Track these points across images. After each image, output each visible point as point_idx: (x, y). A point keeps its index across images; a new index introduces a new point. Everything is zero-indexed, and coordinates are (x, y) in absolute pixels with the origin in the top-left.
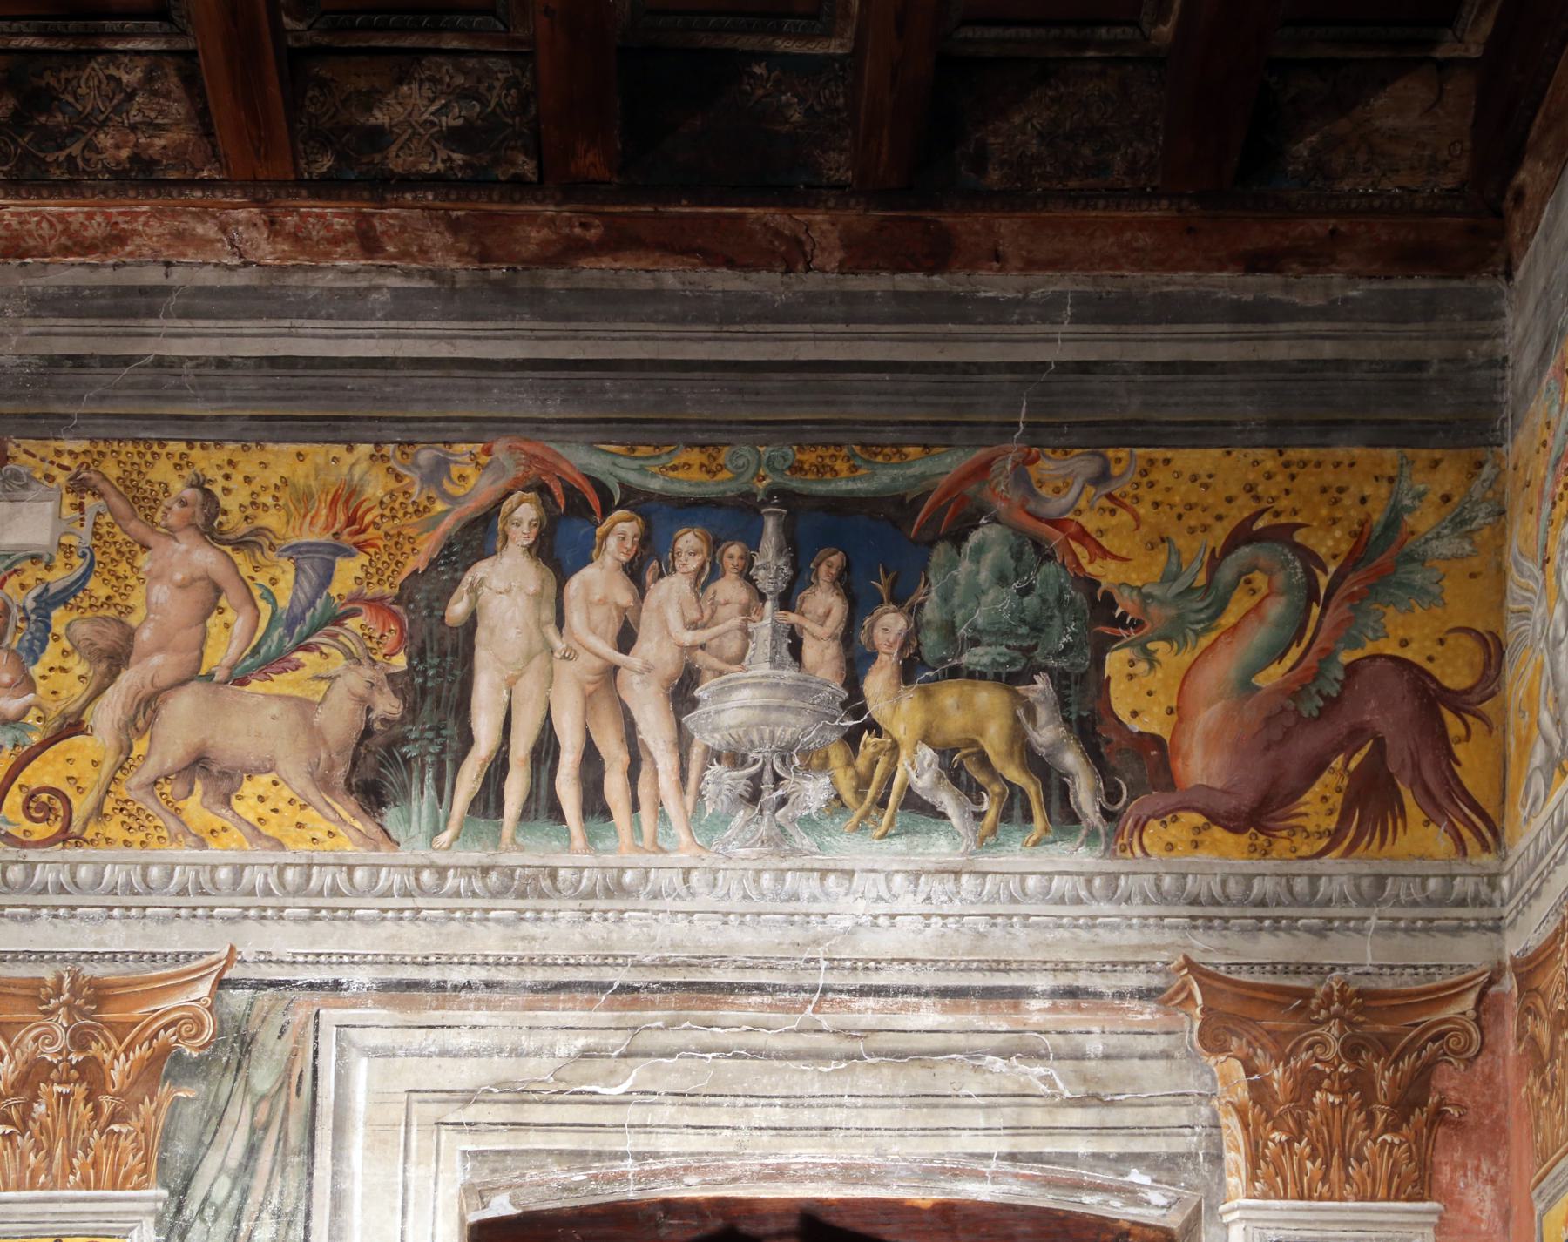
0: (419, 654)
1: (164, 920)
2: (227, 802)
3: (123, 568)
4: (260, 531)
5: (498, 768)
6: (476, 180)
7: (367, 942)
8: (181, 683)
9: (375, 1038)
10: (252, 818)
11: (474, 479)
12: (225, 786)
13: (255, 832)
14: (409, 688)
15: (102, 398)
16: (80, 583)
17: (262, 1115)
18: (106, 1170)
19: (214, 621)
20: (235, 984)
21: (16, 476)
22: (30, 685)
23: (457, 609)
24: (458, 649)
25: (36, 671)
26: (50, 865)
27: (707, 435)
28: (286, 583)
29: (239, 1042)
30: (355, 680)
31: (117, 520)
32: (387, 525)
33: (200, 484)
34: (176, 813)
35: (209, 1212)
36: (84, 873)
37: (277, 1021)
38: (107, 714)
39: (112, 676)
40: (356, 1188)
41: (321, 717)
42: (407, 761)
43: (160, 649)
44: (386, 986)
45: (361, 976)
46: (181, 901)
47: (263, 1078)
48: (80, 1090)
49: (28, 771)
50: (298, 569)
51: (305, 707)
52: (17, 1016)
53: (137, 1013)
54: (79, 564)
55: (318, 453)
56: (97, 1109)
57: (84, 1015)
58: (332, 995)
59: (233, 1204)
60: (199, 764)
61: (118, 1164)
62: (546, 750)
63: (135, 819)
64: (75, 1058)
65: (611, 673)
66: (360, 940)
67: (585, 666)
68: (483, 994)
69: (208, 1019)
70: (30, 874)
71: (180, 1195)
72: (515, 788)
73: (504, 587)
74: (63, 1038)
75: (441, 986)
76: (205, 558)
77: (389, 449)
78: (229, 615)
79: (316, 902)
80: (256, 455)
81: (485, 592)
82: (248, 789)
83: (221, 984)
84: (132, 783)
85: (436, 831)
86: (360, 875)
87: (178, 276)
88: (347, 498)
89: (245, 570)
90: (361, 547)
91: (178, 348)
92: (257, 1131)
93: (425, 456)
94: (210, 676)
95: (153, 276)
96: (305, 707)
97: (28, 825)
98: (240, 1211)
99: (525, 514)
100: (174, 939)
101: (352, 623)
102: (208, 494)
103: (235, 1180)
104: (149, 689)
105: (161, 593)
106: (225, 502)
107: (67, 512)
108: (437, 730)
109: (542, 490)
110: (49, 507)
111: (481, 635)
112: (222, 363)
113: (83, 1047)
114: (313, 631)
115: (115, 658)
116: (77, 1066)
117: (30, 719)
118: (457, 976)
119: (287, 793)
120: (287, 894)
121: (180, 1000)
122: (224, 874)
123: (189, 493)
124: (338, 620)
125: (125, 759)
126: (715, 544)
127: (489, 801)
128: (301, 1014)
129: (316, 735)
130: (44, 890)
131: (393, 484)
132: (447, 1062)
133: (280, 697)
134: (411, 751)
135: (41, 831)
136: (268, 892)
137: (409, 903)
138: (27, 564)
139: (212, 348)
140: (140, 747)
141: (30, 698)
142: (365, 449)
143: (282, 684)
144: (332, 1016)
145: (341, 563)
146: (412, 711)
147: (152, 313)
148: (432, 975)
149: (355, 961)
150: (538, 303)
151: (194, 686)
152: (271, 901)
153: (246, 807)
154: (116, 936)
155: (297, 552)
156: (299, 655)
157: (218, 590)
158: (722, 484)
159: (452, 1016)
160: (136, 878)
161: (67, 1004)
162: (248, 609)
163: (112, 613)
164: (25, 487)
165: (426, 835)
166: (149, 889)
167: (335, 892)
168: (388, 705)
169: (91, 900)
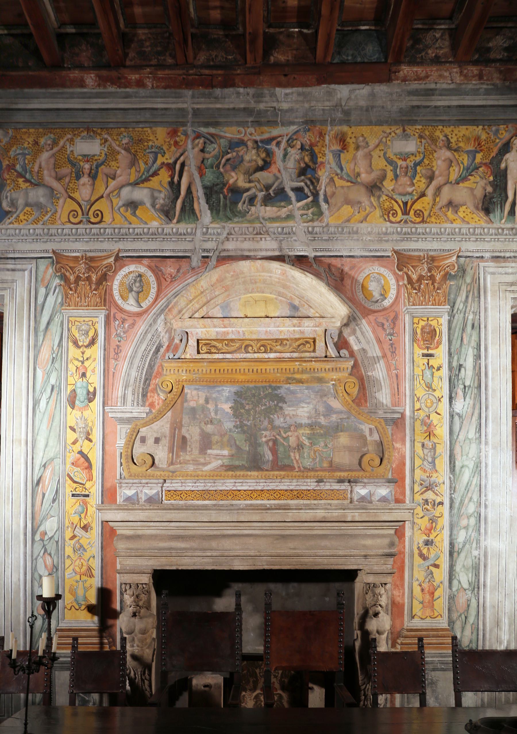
0: (495, 177)
1: (445, 241)
2: (457, 213)
3: (431, 157)
4: (459, 147)
8: (445, 184)
9: (491, 270)
10: (462, 216)
12: (456, 209)
13: (463, 220)
15: (424, 116)
16: (422, 161)
17: (469, 289)
18: (437, 301)
19: (451, 169)
20: (461, 257)
21: (407, 134)
22: (413, 185)
23: (503, 166)
25: (415, 181)
28: (465, 159)
29: (463, 271)
30: (482, 183)
31: (429, 145)
32: (486, 145)
33: (446, 136)
34: (446, 215)
35: (459, 312)
36: (428, 230)
37: (471, 266)
38: (430, 192)
39: (430, 182)
40: (489, 307)
41: (475, 192)
42: (494, 203)
43: (440, 176)
44: (493, 257)
45: (487, 255)
46: (449, 237)
47: (468, 280)
48: (430, 282)
49: (414, 206)
50: (468, 156)
51: (472, 190)
52: (416, 264)
53: (441, 264)
54: (422, 155)
55: (471, 128)
56: (434, 287)
57: (430, 264)
58: (481, 260)
59: (464, 310)
61: (439, 300)
63: (438, 217)
64: (429, 274)
66: (487, 246)
68: (513, 259)
69: (456, 265)
70: (416, 230)
71: (453, 307)
74: (426, 269)
75: (504, 257)
76: (448, 154)
77: (486, 127)
78: (454, 168)
79: (477, 237)
80: (457, 129)
81: (509, 161)
82: (462, 209)
83: (458, 257)
84: (436, 209)
85: (501, 220)
86: (486, 230)
87: (438, 86)
88: (477, 139)
89: (457, 157)
90: (481, 151)
91: (439, 103)
92: (468, 292)
93: (494, 128)
94: (451, 182)
95: (433, 86)
96: (472, 190)
97: (415, 218)
98: (465, 311)
100: (448, 246)
101: (481, 169)
102: (448, 139)
103: (464, 304)
104: (438, 186)
105: (440, 162)
106: (452, 140)
107: (419, 143)
108: (500, 195)
110: (415, 142)
111: (508, 172)
112: (449, 107)
113: (430, 272)
114: (472, 171)
115: (431, 178)
116: (430, 276)
117: (414, 193)
118: (508, 255)
119: (469, 211)
120: (471, 235)
121: (450, 261)
122: (457, 230)
123: (444, 138)
124: (477, 168)
128: (475, 264)
129: (474, 196)
130: (419, 234)
131: (487, 135)
132: (506, 276)
133: (467, 187)
134: (495, 200)
135: (418, 220)
136: (467, 235)
137: (496, 237)
138: (411, 156)
139: (446, 103)
140: (438, 199)
141: (414, 188)
142: (481, 127)
143: (466, 184)
144: (482, 264)
145: (477, 155)
146: (495, 190)
147: (433, 95)
148: (502, 254)
149: (487, 251)
151: (448, 185)
152: (467, 237)
153: (461, 214)
154: (435, 245)
155: (468, 152)
156: (470, 177)
157: (451, 162)
159: (507, 264)
160: (439, 231)
161: (427, 261)
162: (458, 166)
163: (429, 167)
164: (409, 137)
165: (499, 221)
166: (442, 234)
167: (481, 234)
168: (489, 189)
169: (430, 236)
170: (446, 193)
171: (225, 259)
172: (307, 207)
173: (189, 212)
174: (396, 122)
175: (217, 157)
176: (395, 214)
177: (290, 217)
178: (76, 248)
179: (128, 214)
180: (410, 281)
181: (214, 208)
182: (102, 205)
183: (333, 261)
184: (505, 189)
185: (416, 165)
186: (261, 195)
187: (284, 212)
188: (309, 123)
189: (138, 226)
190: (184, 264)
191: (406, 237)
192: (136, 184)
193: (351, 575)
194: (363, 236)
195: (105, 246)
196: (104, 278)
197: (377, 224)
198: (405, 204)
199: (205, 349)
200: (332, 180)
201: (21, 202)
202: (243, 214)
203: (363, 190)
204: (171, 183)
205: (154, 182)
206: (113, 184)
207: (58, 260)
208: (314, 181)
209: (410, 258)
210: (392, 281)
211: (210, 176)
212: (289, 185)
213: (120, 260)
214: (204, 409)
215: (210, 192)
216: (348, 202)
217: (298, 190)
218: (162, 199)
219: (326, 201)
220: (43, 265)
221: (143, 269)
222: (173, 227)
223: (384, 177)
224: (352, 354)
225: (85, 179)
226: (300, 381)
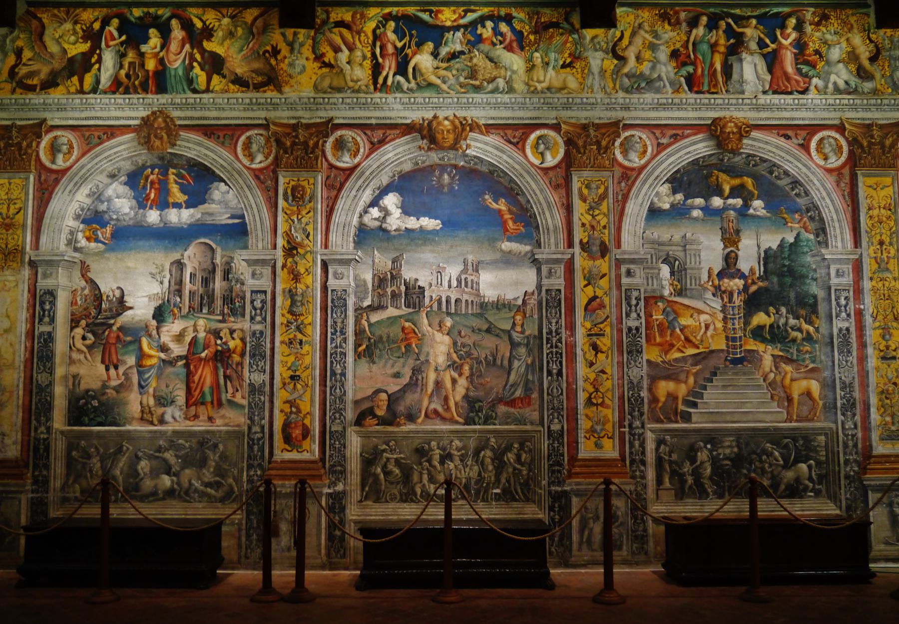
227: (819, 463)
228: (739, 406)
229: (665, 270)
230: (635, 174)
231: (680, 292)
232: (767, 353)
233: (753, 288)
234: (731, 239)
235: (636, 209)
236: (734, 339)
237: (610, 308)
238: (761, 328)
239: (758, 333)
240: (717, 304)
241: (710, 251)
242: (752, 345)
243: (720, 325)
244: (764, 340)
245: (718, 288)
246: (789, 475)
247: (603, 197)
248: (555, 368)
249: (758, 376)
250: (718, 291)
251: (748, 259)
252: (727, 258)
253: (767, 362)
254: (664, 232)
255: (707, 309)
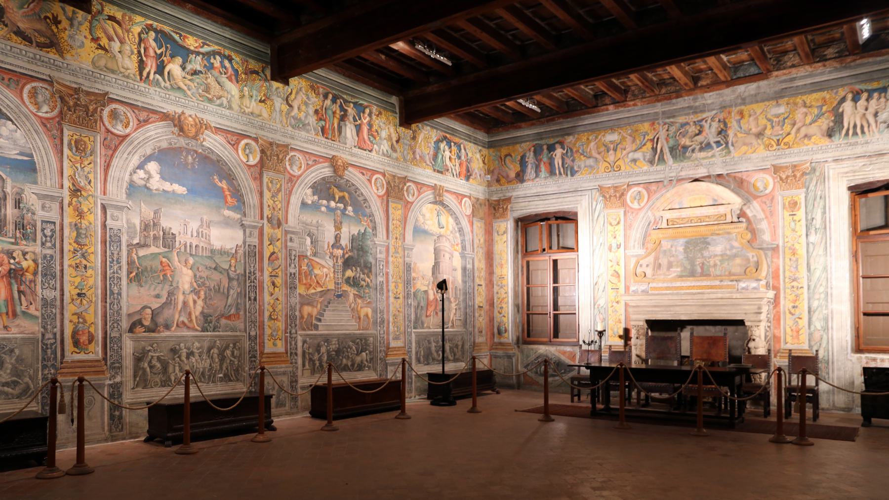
5: (848, 130)
6: (840, 56)
7: (830, 155)
11: (841, 93)
13: (814, 143)
14: (835, 122)
23: (841, 110)
24: (842, 114)
26: (787, 151)
27: (878, 80)
28: (816, 111)
30: (827, 122)
51: (820, 126)
60: (806, 136)
62: (855, 126)
65: (864, 114)
66: (830, 155)
67: (861, 114)
72: (851, 132)
73: (848, 106)
82: (813, 138)
99: (850, 96)
100: (804, 158)
109: (852, 92)
115: (794, 125)
125: (796, 137)
126: (880, 94)
127: (847, 134)
143: (816, 124)
150: (850, 68)
154: (797, 159)
158: (881, 86)
165: (838, 140)
168: (832, 124)
170: (803, 131)
171: (680, 180)
172: (722, 150)
173: (662, 159)
174: (772, 99)
175: (675, 132)
176: (772, 146)
177: (713, 156)
178: (608, 183)
179: (633, 165)
180: (781, 179)
181: (674, 157)
182: (620, 163)
183: (737, 175)
184: (842, 123)
185: (784, 119)
186: (698, 147)
187: (710, 154)
188: (723, 108)
189: (637, 170)
190: (660, 185)
191: (779, 157)
192: (636, 151)
193: (741, 323)
194: (752, 160)
195: (623, 180)
196: (623, 194)
197: (762, 152)
198: (778, 140)
199: (670, 223)
200: (736, 135)
201: (583, 166)
202: (689, 158)
203: (753, 137)
204: (653, 148)
205: (644, 149)
206: (624, 152)
207: (601, 189)
208: (726, 137)
209: (781, 167)
210: (771, 180)
211: (671, 142)
212: (712, 139)
213: (629, 186)
214: (670, 250)
215: (672, 150)
216: (745, 144)
217: (718, 143)
218: (648, 156)
219: (733, 145)
220: (594, 192)
221: (640, 189)
222: (655, 168)
223: (765, 128)
224: (749, 221)
225: (611, 152)
226: (718, 234)
227: (370, 352)
228: (339, 321)
229: (308, 240)
230: (295, 179)
231: (315, 254)
232: (352, 291)
233: (347, 256)
234: (338, 227)
235: (295, 201)
236: (338, 284)
237: (281, 262)
238: (349, 278)
239: (348, 281)
240: (331, 263)
241: (328, 233)
242: (346, 287)
243: (332, 275)
244: (350, 285)
245: (331, 253)
246: (358, 359)
247: (279, 190)
248: (252, 295)
249: (347, 305)
250: (332, 256)
251: (345, 242)
252: (336, 237)
253: (351, 297)
254: (310, 218)
255: (326, 265)
